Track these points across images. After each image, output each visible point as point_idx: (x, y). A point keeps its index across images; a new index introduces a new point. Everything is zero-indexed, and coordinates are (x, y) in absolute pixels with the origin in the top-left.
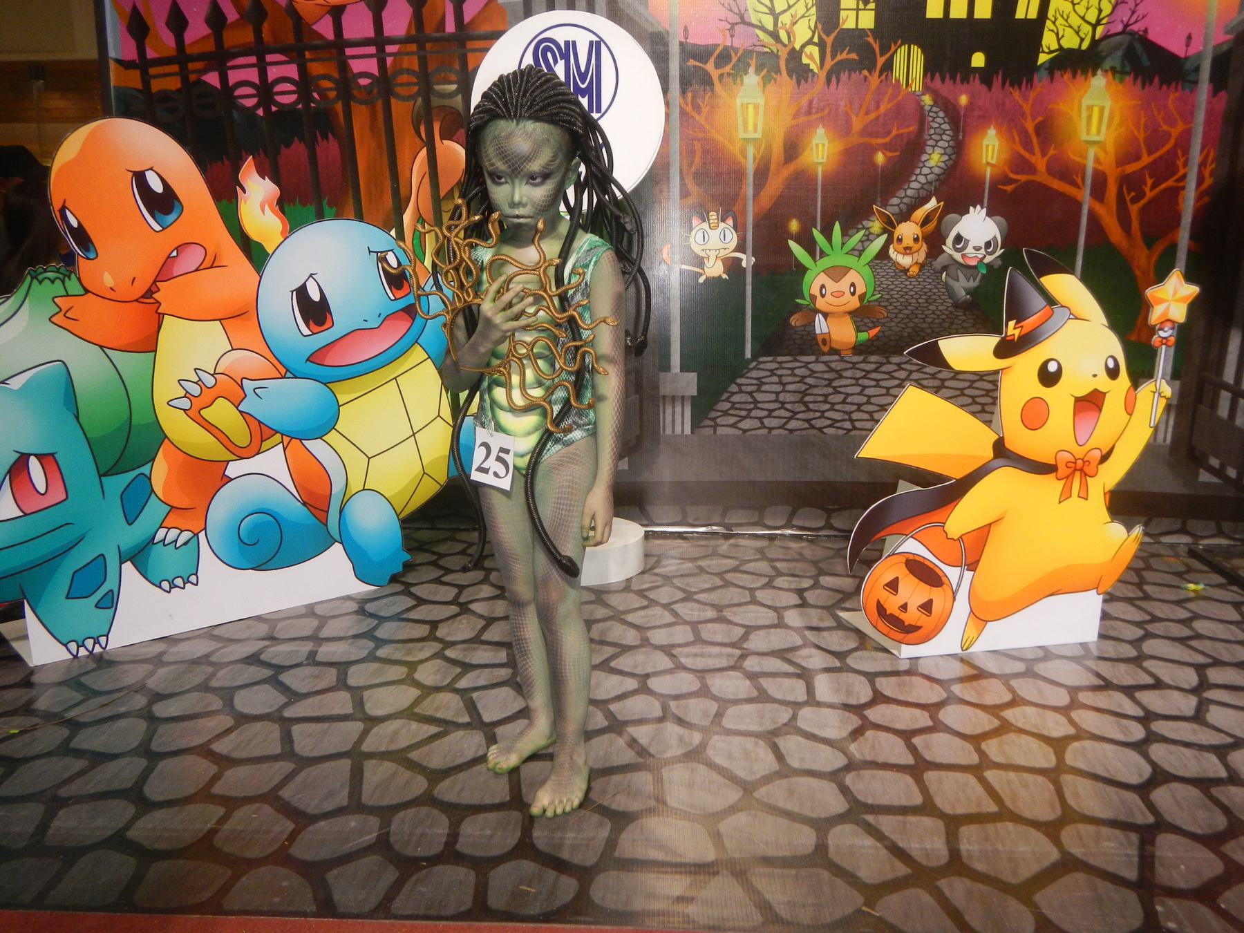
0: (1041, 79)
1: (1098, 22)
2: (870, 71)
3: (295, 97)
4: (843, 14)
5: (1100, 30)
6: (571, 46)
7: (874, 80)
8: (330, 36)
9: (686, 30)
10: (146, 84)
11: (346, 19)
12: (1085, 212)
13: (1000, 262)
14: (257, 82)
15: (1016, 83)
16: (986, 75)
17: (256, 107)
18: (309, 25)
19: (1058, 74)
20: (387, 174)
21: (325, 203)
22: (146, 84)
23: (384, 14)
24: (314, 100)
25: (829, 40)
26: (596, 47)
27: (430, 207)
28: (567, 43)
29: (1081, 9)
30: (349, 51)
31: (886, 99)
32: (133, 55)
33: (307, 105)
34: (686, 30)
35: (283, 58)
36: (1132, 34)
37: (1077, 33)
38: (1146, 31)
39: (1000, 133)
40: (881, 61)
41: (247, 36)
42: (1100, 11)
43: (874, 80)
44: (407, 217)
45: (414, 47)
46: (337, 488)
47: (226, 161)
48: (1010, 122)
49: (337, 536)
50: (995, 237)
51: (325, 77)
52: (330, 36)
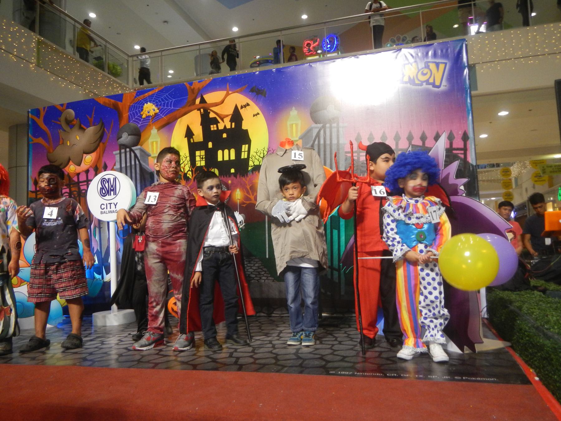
0: (250, 174)
4: (197, 162)
6: (109, 179)
10: (36, 196)
11: (80, 176)
13: (244, 227)
15: (243, 176)
16: (235, 175)
18: (72, 179)
19: (254, 172)
22: (36, 196)
25: (194, 170)
26: (115, 179)
29: (259, 154)
30: (81, 184)
32: (34, 190)
35: (66, 187)
39: (240, 190)
42: (264, 154)
44: (92, 226)
48: (243, 187)
50: (242, 220)
51: (75, 191)
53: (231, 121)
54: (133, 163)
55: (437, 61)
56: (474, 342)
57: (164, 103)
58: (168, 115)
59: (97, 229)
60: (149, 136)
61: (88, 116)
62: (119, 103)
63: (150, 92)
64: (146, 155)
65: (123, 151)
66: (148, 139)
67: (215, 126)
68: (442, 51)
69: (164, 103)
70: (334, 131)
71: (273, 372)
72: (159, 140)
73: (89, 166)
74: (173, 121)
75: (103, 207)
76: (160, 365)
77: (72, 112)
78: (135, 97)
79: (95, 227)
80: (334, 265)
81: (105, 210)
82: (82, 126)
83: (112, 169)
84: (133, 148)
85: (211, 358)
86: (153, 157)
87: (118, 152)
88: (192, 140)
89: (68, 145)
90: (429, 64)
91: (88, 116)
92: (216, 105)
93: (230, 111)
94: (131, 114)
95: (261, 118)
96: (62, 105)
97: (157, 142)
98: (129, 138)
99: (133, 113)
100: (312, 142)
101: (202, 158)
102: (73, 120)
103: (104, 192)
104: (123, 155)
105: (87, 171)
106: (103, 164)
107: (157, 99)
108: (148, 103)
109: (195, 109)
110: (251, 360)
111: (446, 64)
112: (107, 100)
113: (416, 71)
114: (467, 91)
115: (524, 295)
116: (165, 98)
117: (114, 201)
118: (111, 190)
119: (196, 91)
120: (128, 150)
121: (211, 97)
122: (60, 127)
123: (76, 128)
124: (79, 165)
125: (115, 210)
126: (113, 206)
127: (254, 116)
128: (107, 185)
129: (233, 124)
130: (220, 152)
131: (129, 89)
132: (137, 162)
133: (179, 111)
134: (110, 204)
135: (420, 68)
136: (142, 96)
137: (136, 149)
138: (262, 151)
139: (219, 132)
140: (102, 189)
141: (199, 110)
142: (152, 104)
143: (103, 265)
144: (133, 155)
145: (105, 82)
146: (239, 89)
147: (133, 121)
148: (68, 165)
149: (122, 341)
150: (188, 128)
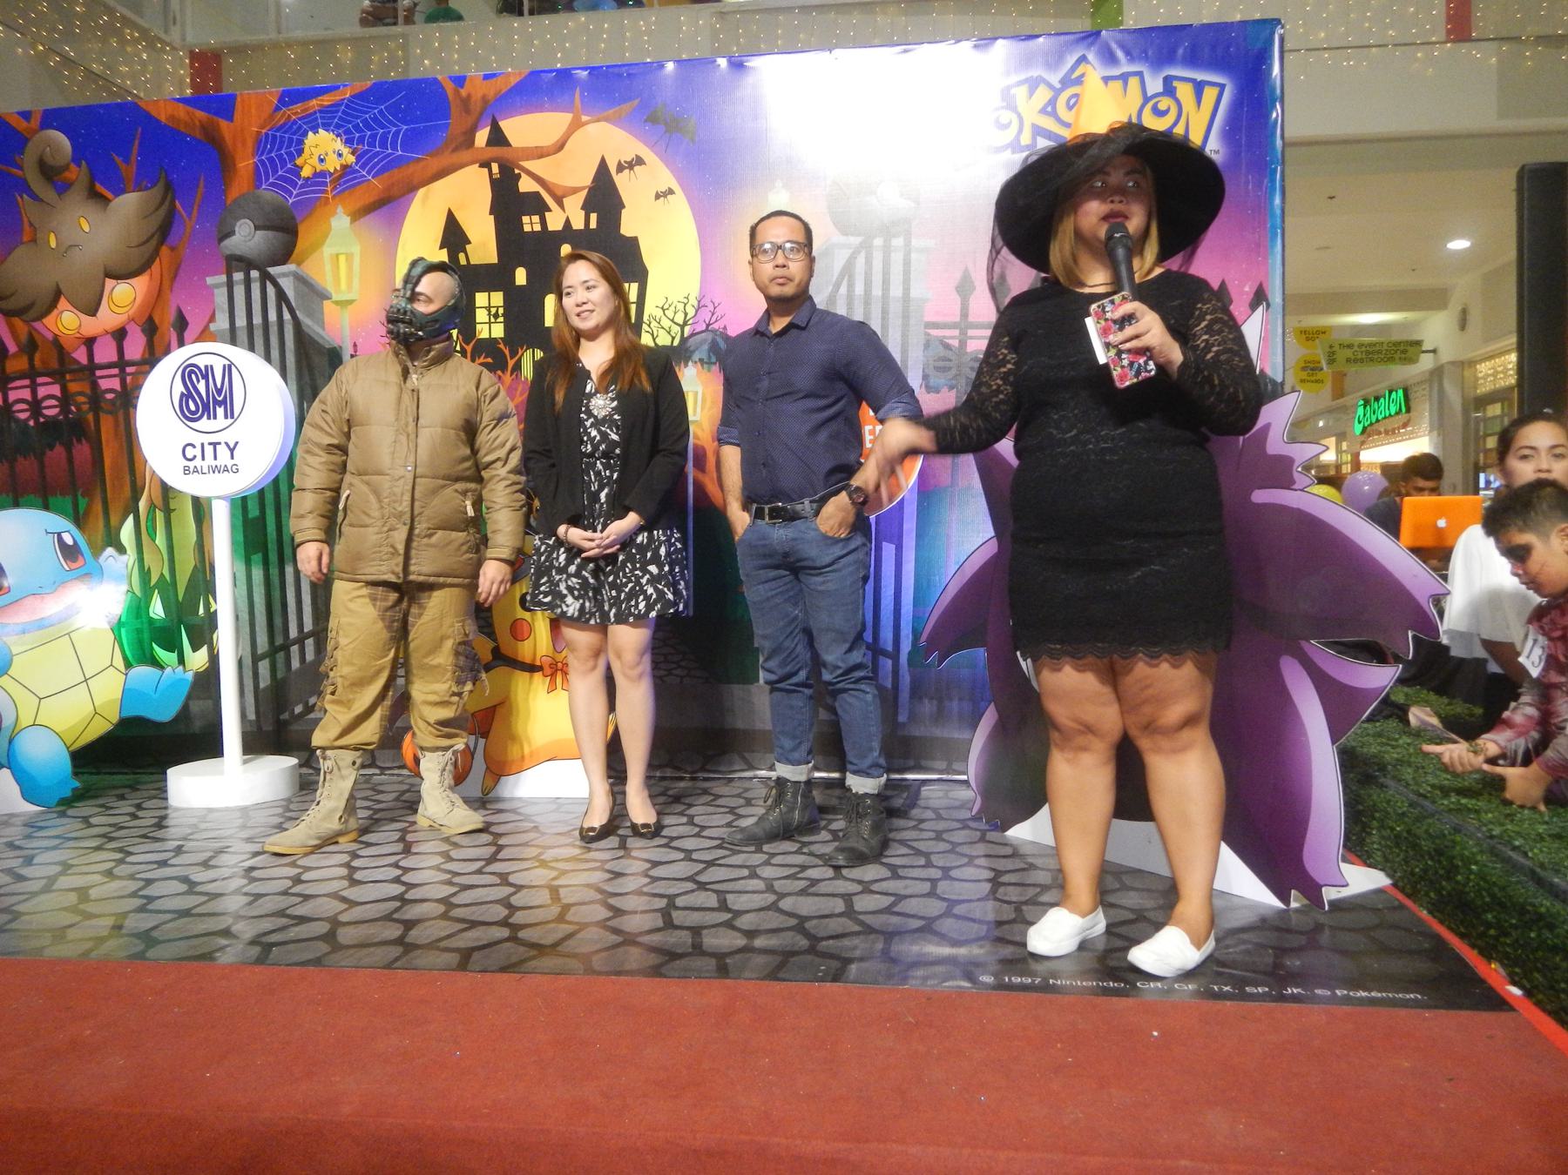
1: (685, 323)
2: (503, 372)
3: (56, 411)
4: (478, 327)
5: (687, 330)
7: (507, 378)
8: (84, 360)
9: (355, 345)
11: (97, 348)
12: (691, 481)
14: (29, 399)
17: (27, 420)
18: (69, 354)
20: (127, 469)
21: (79, 494)
23: (126, 344)
24: (70, 411)
25: (469, 348)
26: (228, 369)
27: (160, 498)
28: (206, 367)
29: (670, 313)
30: (98, 373)
31: (518, 392)
33: (66, 417)
34: (355, 345)
35: (50, 380)
36: (714, 331)
37: (669, 333)
38: (725, 328)
40: (511, 363)
41: (20, 364)
42: (686, 314)
43: (507, 378)
44: (142, 504)
45: (147, 367)
46: (8, 722)
47: (5, 464)
49: (6, 765)
51: (81, 393)
52: (84, 360)
53: (588, 207)
54: (273, 316)
55: (1200, 76)
56: (1322, 883)
57: (373, 137)
58: (386, 175)
59: (159, 515)
60: (326, 237)
61: (118, 160)
62: (223, 123)
63: (325, 97)
64: (314, 293)
65: (238, 276)
66: (323, 243)
67: (536, 219)
68: (1214, 48)
69: (373, 137)
70: (897, 259)
71: (822, 980)
72: (356, 250)
73: (124, 318)
74: (403, 195)
75: (190, 452)
76: (476, 956)
77: (60, 141)
78: (277, 109)
79: (152, 506)
80: (881, 642)
81: (198, 462)
82: (99, 187)
83: (204, 336)
84: (272, 270)
85: (616, 931)
86: (337, 303)
87: (223, 278)
88: (462, 256)
89: (53, 244)
90: (1175, 84)
91: (118, 160)
92: (540, 153)
93: (585, 177)
94: (262, 162)
95: (679, 204)
96: (26, 115)
97: (349, 257)
98: (256, 238)
99: (271, 160)
100: (830, 288)
101: (496, 316)
102: (66, 168)
103: (193, 407)
104: (239, 291)
105: (120, 334)
106: (171, 316)
107: (350, 122)
108: (320, 130)
109: (472, 163)
110: (741, 942)
111: (1222, 87)
112: (182, 111)
113: (1139, 101)
114: (1276, 169)
115: (1396, 740)
116: (375, 119)
117: (227, 437)
118: (217, 403)
119: (476, 106)
120: (255, 274)
121: (523, 129)
122: (24, 187)
123: (76, 195)
124: (94, 314)
125: (230, 463)
126: (222, 450)
127: (658, 197)
128: (201, 386)
129: (594, 217)
130: (550, 301)
131: (173, 48)
132: (287, 316)
133: (422, 164)
134: (215, 445)
135: (1149, 95)
136: (298, 108)
137: (284, 275)
138: (680, 306)
139: (547, 241)
140: (186, 397)
141: (486, 164)
142: (331, 135)
143: (180, 622)
144: (271, 290)
145: (96, 22)
146: (611, 111)
147: (272, 185)
148: (55, 312)
149: (308, 869)
150: (450, 215)
